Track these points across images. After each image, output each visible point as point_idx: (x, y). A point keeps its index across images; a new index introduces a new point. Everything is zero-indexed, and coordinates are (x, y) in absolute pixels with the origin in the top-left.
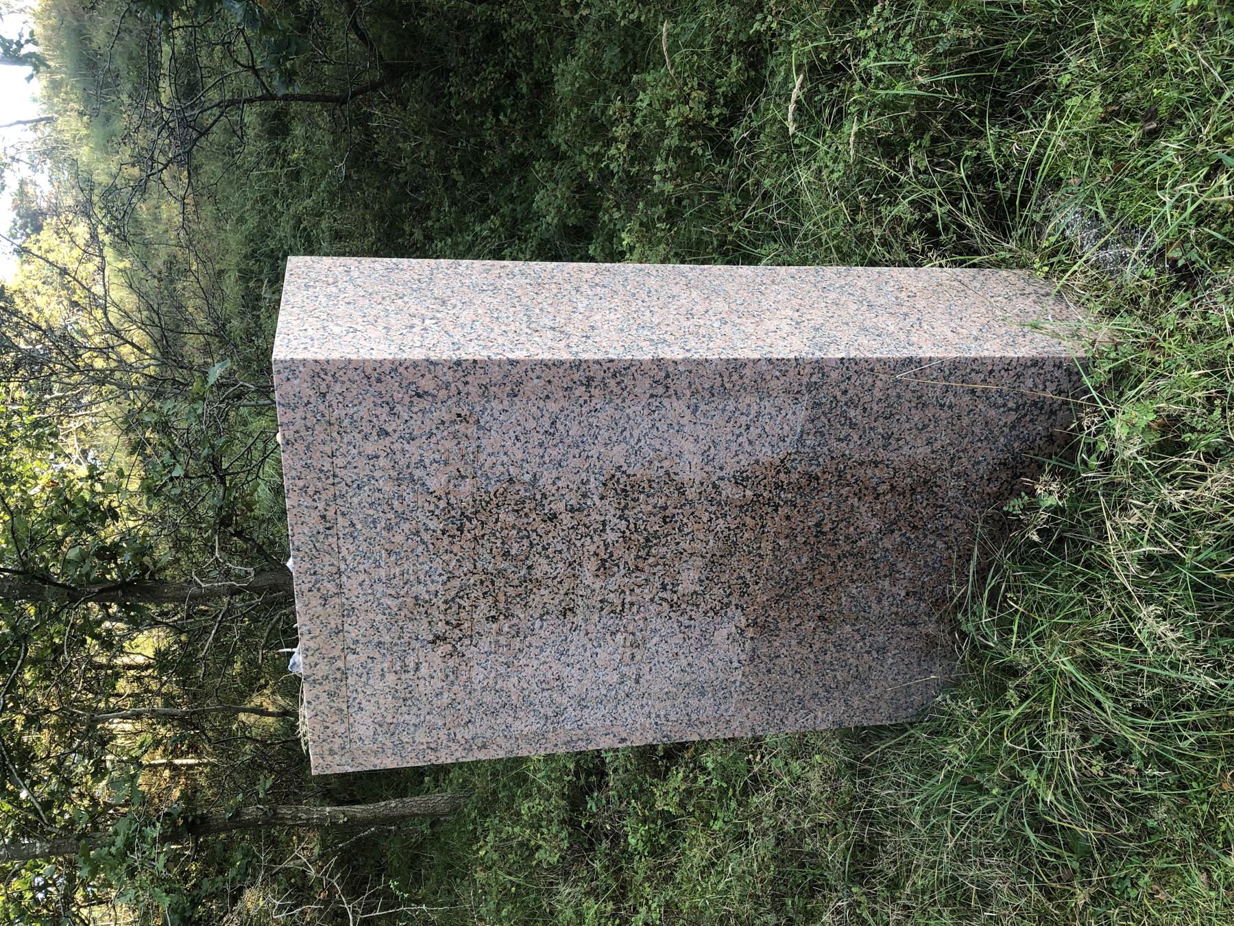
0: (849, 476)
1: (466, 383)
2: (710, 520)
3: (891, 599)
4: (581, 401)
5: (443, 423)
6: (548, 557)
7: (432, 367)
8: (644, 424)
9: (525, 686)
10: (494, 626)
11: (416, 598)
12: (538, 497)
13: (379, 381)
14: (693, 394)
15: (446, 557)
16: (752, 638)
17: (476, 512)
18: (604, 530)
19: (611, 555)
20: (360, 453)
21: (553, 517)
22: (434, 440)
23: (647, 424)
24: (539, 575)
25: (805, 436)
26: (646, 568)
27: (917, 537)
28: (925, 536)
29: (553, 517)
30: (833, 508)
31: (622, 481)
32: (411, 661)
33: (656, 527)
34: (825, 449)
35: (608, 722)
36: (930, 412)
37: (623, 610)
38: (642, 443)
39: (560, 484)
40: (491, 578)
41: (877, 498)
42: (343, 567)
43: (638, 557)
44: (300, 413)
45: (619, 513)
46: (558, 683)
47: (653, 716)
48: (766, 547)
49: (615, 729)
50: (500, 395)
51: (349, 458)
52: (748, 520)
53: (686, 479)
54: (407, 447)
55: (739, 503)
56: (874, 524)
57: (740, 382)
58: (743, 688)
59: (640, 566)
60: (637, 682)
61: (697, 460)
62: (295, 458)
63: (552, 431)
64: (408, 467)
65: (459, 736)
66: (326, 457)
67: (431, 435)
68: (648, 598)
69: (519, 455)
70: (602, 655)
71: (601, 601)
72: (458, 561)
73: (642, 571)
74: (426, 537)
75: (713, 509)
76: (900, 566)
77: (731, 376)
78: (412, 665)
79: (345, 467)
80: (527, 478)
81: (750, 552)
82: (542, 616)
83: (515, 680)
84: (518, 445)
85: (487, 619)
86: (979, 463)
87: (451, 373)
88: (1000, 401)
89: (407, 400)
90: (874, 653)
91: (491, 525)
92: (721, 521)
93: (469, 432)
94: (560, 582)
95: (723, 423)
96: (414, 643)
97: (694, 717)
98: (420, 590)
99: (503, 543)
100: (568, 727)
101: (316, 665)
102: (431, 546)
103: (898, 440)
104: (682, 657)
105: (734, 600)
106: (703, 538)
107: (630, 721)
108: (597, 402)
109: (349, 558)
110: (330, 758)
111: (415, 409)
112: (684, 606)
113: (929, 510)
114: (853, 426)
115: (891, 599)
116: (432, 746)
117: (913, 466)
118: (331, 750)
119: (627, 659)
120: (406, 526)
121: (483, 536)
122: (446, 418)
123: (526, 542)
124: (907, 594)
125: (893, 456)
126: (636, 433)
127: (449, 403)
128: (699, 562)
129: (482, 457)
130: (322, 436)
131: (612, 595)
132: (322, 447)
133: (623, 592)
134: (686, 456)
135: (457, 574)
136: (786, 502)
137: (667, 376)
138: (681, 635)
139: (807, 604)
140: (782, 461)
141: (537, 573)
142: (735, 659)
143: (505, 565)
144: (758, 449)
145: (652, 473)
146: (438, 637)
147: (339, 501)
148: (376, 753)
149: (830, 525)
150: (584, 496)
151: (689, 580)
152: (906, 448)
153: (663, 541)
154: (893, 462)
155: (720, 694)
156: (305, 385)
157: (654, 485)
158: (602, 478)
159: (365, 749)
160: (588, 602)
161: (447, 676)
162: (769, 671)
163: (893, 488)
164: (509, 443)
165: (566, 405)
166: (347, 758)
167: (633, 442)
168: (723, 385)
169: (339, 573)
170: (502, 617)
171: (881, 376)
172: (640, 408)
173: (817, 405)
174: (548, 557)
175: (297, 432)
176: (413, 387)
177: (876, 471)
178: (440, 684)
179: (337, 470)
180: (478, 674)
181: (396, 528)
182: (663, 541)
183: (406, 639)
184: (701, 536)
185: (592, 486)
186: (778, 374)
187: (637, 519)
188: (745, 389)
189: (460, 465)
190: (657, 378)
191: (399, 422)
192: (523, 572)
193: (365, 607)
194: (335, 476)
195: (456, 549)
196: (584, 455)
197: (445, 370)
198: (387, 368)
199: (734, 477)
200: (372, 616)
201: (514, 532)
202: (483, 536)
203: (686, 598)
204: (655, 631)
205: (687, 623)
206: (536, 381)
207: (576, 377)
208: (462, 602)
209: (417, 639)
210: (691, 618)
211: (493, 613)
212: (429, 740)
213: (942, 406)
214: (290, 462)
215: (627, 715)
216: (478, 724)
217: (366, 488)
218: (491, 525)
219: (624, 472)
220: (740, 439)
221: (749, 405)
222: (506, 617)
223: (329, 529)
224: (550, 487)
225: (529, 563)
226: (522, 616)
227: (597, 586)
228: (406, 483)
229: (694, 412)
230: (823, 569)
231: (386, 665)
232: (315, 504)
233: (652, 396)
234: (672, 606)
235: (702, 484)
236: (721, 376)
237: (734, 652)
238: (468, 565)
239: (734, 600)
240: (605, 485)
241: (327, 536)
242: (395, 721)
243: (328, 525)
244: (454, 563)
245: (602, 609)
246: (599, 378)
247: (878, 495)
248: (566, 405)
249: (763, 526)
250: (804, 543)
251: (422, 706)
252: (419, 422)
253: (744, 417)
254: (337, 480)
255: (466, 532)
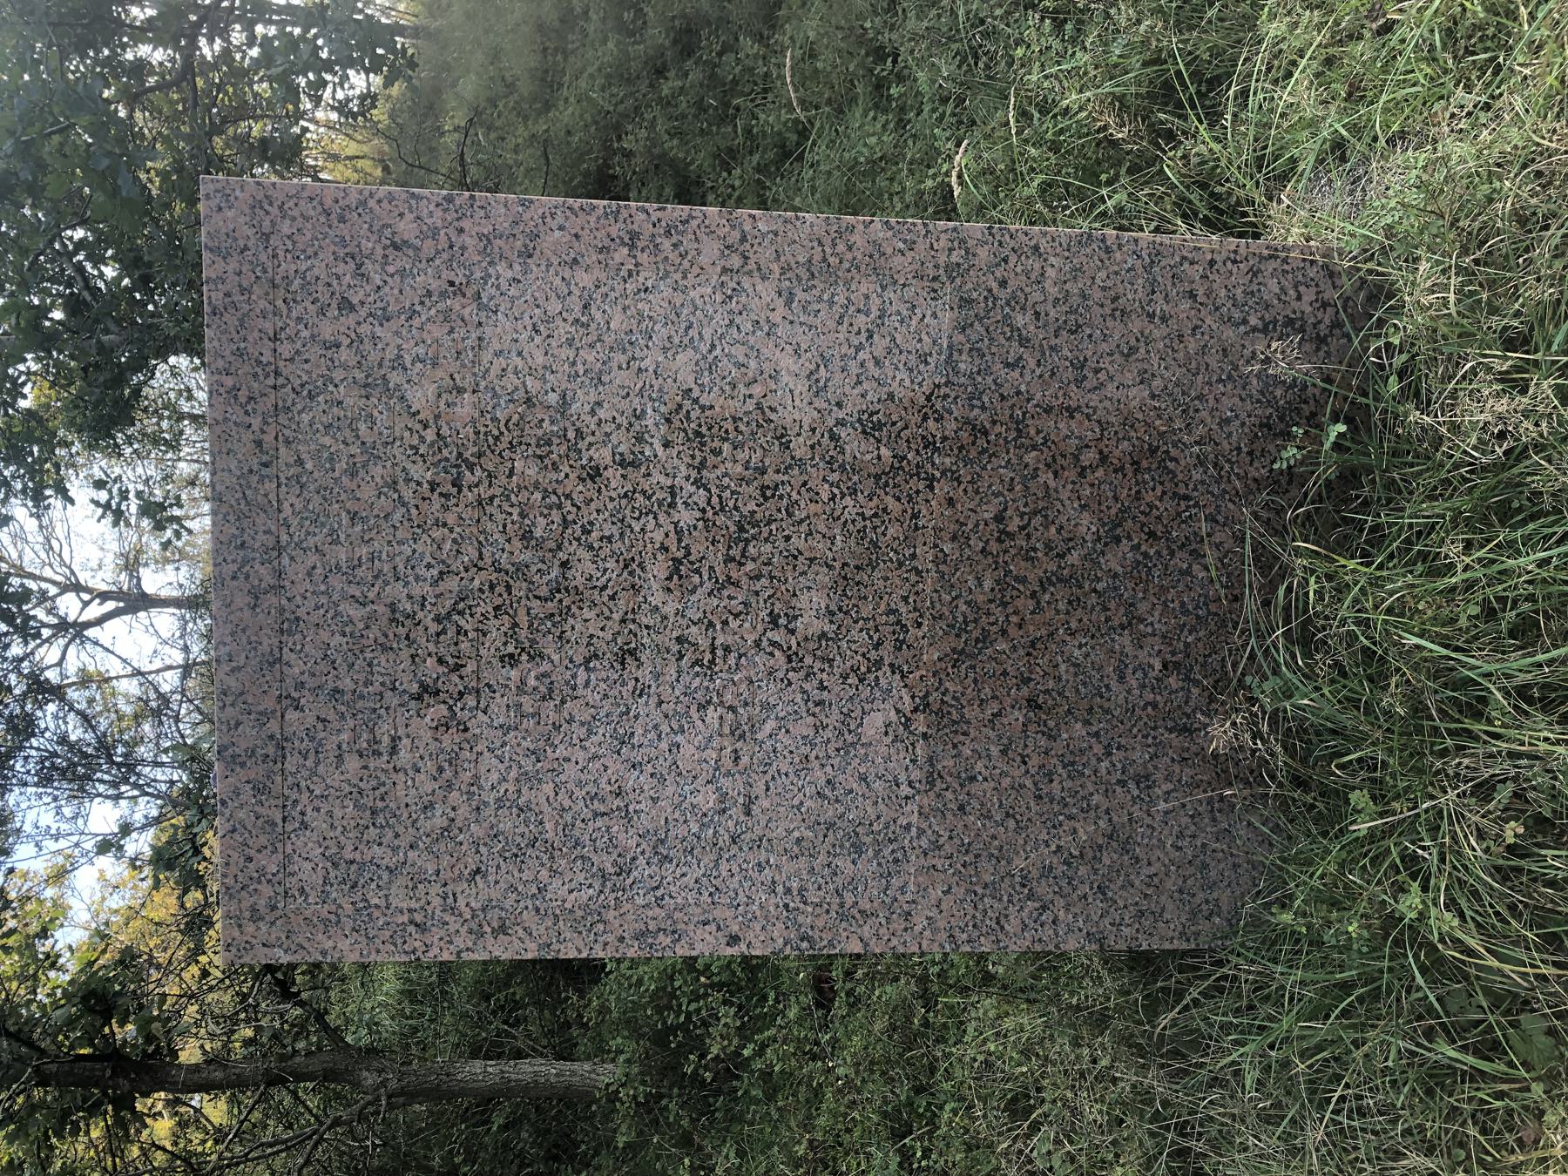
0: (1032, 432)
1: (461, 231)
2: (833, 499)
3: (1139, 674)
4: (624, 273)
5: (429, 294)
6: (591, 548)
7: (413, 202)
8: (718, 317)
9: (567, 803)
10: (514, 674)
11: (393, 607)
12: (571, 435)
13: (342, 220)
14: (783, 271)
15: (437, 533)
16: (925, 736)
17: (480, 455)
18: (672, 505)
19: (688, 554)
20: (313, 337)
21: (595, 473)
22: (416, 322)
23: (721, 319)
24: (580, 581)
25: (956, 356)
26: (744, 580)
27: (1158, 553)
28: (1172, 553)
29: (595, 473)
30: (1018, 488)
31: (693, 415)
32: (384, 730)
33: (752, 506)
34: (989, 380)
35: (705, 897)
36: (1136, 325)
37: (712, 662)
38: (717, 352)
39: (602, 414)
40: (508, 577)
41: (1082, 474)
42: (284, 538)
43: (729, 559)
44: (233, 266)
45: (694, 474)
46: (618, 802)
47: (780, 889)
48: (925, 556)
49: (717, 913)
50: (509, 254)
51: (298, 345)
52: (890, 502)
53: (789, 420)
54: (379, 331)
55: (873, 470)
56: (1087, 525)
57: (849, 256)
58: (924, 843)
59: (734, 575)
60: (748, 813)
61: (801, 387)
62: (224, 338)
63: (584, 319)
64: (380, 365)
65: (461, 903)
66: (266, 341)
67: (413, 313)
68: (751, 639)
69: (540, 359)
70: (688, 750)
71: (679, 640)
72: (455, 541)
73: (736, 584)
74: (407, 494)
75: (835, 477)
76: (1142, 608)
77: (834, 245)
78: (386, 740)
79: (291, 360)
80: (553, 398)
81: (901, 565)
82: (588, 660)
83: (548, 788)
84: (538, 340)
85: (502, 659)
86: (1228, 421)
87: (439, 213)
88: (1237, 315)
89: (379, 251)
90: (1131, 785)
91: (503, 480)
92: (848, 501)
93: (466, 311)
94: (612, 598)
95: (831, 324)
96: (392, 699)
97: (849, 898)
98: (396, 591)
99: (523, 515)
100: (640, 901)
101: (238, 724)
102: (414, 511)
103: (1097, 371)
104: (815, 764)
105: (886, 652)
106: (824, 530)
107: (742, 898)
108: (647, 276)
109: (295, 522)
110: (250, 928)
111: (391, 269)
112: (808, 660)
113: (1169, 504)
114: (1024, 342)
115: (1139, 674)
116: (418, 918)
117: (1128, 422)
118: (254, 910)
119: (727, 762)
120: (377, 471)
121: (492, 498)
122: (435, 285)
123: (556, 516)
124: (1165, 666)
125: (1094, 399)
126: (707, 333)
127: (437, 262)
128: (824, 577)
129: (487, 356)
130: (262, 304)
131: (694, 629)
132: (260, 323)
133: (711, 625)
134: (785, 378)
135: (453, 568)
136: (943, 473)
137: (743, 239)
138: (810, 720)
139: (1005, 674)
140: (928, 399)
141: (577, 578)
142: (902, 778)
143: (526, 556)
144: (890, 374)
145: (735, 406)
146: (424, 687)
147: (283, 419)
148: (326, 922)
149: (1017, 521)
150: (639, 439)
151: (811, 618)
152: (1110, 389)
153: (765, 530)
154: (1095, 409)
155: (887, 852)
156: (242, 220)
157: (742, 427)
158: (663, 409)
159: (308, 913)
160: (658, 639)
161: (441, 770)
162: (961, 808)
163: (1104, 458)
164: (524, 336)
165: (603, 276)
166: (277, 933)
167: (704, 348)
168: (824, 260)
169: (279, 548)
170: (524, 657)
171: (1052, 260)
172: (709, 290)
173: (966, 302)
174: (591, 548)
175: (227, 295)
176: (388, 232)
177: (1073, 424)
178: (429, 786)
179: (281, 364)
180: (491, 770)
181: (362, 473)
182: (765, 530)
183: (377, 687)
184: (822, 528)
185: (650, 422)
186: (901, 245)
187: (723, 488)
188: (858, 268)
189: (454, 367)
190: (730, 241)
191: (368, 288)
192: (555, 572)
193: (314, 618)
194: (277, 374)
195: (451, 519)
196: (635, 365)
197: (432, 207)
198: (353, 199)
199: (859, 420)
200: (324, 635)
201: (538, 496)
202: (492, 498)
203: (812, 645)
204: (767, 707)
205: (816, 694)
206: (557, 233)
207: (614, 232)
208: (462, 623)
209: (394, 689)
210: (822, 688)
211: (510, 649)
212: (414, 904)
213: (1151, 316)
214: (216, 343)
215: (734, 883)
216: (491, 878)
217: (321, 399)
218: (503, 480)
219: (696, 401)
220: (861, 356)
221: (867, 297)
222: (531, 658)
223: (266, 465)
224: (588, 418)
225: (562, 556)
226: (555, 657)
227: (669, 609)
228: (376, 393)
229: (789, 303)
230: (1019, 603)
231: (345, 736)
232: (247, 419)
233: (725, 270)
234: (790, 661)
235: (813, 430)
236: (820, 243)
237: (899, 763)
238: (470, 552)
239: (886, 652)
240: (668, 421)
241: (261, 480)
242: (358, 856)
243: (265, 458)
244: (448, 546)
245: (681, 657)
246: (646, 236)
247: (1084, 469)
248: (603, 276)
249: (915, 516)
250: (983, 551)
251: (401, 830)
252: (396, 291)
253: (862, 317)
254: (281, 381)
255: (465, 490)
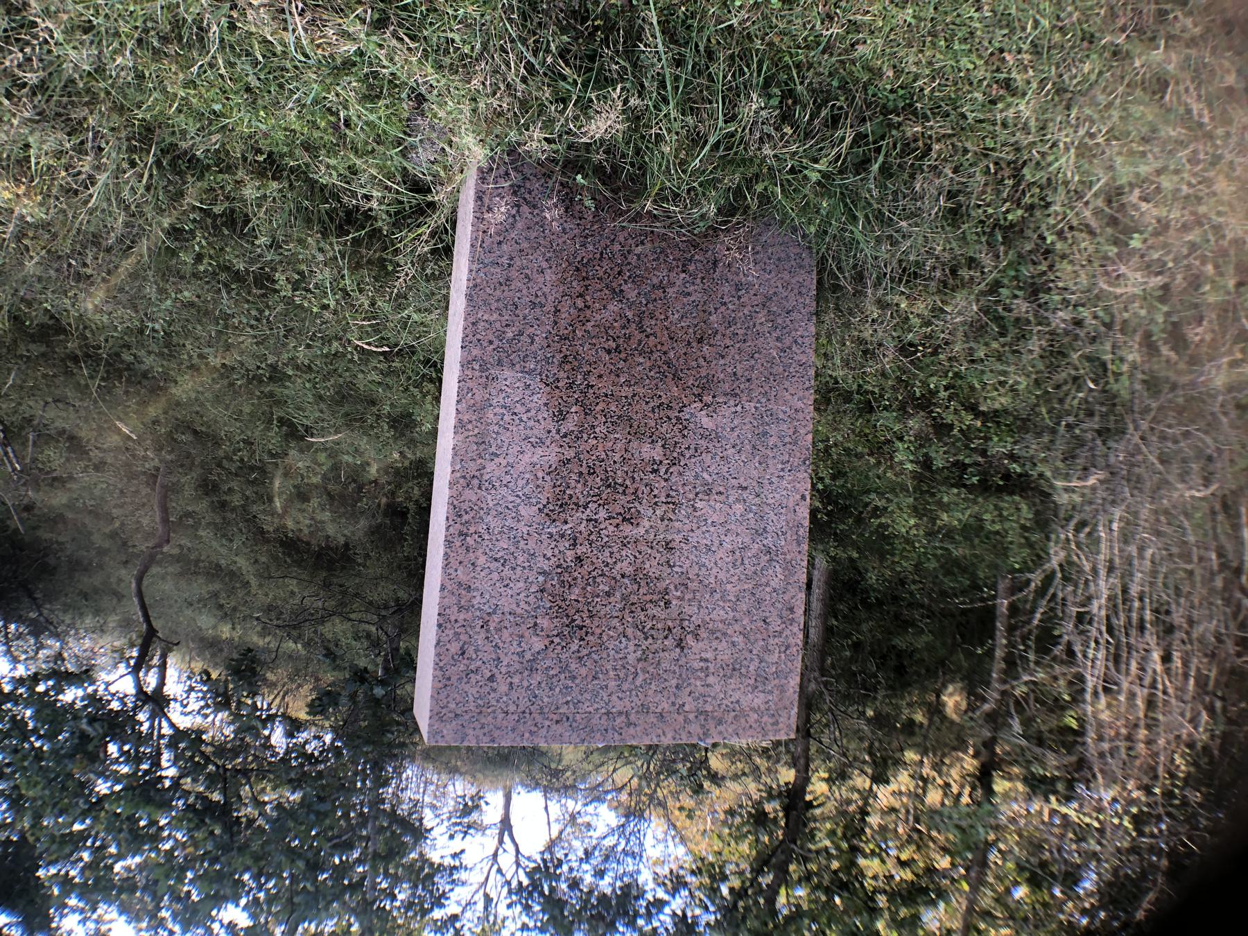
1: (456, 621)
5: (487, 638)
10: (674, 602)
12: (559, 570)
13: (449, 679)
14: (481, 457)
15: (605, 638)
16: (714, 397)
17: (567, 616)
18: (596, 521)
21: (579, 559)
22: (501, 645)
23: (504, 491)
24: (631, 569)
26: (635, 486)
28: (629, 263)
29: (579, 559)
32: (697, 665)
39: (549, 554)
41: (589, 307)
42: (603, 711)
43: (624, 493)
44: (471, 732)
48: (627, 391)
49: (791, 505)
52: (599, 408)
54: (505, 663)
56: (614, 307)
58: (764, 400)
59: (632, 491)
60: (746, 488)
61: (539, 451)
65: (778, 629)
69: (521, 584)
70: (715, 518)
73: (637, 490)
74: (585, 652)
75: (585, 436)
76: (655, 281)
78: (702, 664)
80: (541, 579)
82: (670, 566)
83: (729, 586)
86: (564, 229)
87: (447, 632)
89: (465, 661)
91: (580, 605)
92: (597, 430)
93: (497, 620)
95: (508, 434)
97: (787, 440)
98: (631, 658)
105: (673, 414)
107: (784, 493)
108: (481, 528)
109: (596, 706)
111: (474, 656)
112: (675, 455)
113: (604, 264)
114: (521, 333)
116: (783, 649)
117: (563, 281)
119: (721, 498)
120: (573, 666)
122: (483, 635)
125: (550, 298)
126: (511, 499)
128: (634, 444)
129: (519, 611)
130: (490, 718)
131: (658, 512)
133: (656, 503)
134: (535, 459)
137: (464, 477)
139: (685, 354)
141: (629, 570)
142: (733, 409)
143: (618, 595)
145: (548, 485)
146: (678, 645)
149: (610, 343)
150: (562, 536)
152: (545, 289)
160: (661, 530)
162: (748, 380)
163: (581, 295)
164: (510, 592)
165: (481, 551)
167: (519, 501)
173: (500, 363)
178: (724, 643)
180: (719, 614)
185: (554, 531)
187: (589, 494)
189: (524, 627)
192: (626, 581)
195: (598, 631)
196: (525, 536)
198: (439, 673)
201: (589, 588)
204: (696, 477)
205: (692, 451)
207: (458, 544)
210: (688, 448)
211: (662, 604)
213: (510, 265)
215: (777, 496)
218: (580, 605)
224: (552, 562)
225: (619, 577)
227: (647, 524)
229: (497, 456)
231: (698, 683)
233: (480, 488)
237: (726, 411)
238: (615, 622)
239: (673, 414)
244: (611, 633)
245: (670, 520)
248: (481, 551)
249: (606, 396)
253: (506, 418)
